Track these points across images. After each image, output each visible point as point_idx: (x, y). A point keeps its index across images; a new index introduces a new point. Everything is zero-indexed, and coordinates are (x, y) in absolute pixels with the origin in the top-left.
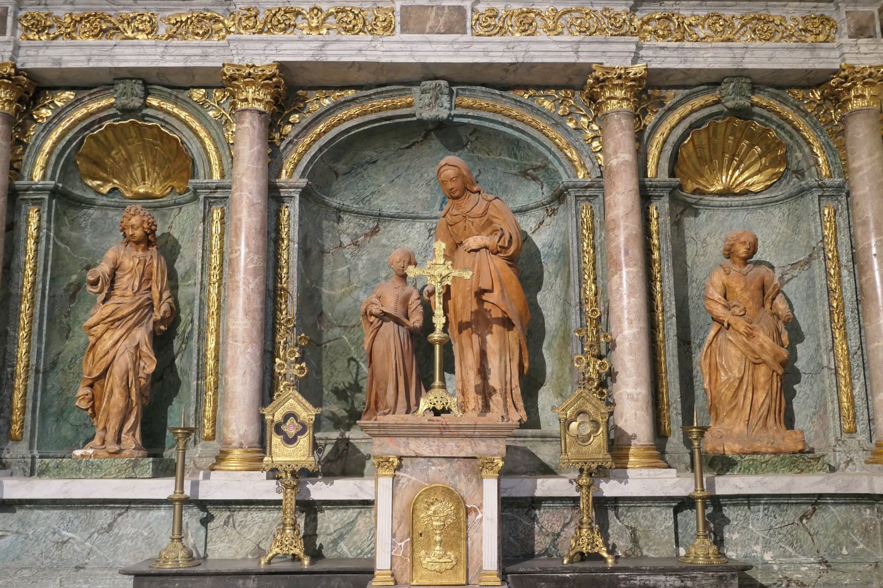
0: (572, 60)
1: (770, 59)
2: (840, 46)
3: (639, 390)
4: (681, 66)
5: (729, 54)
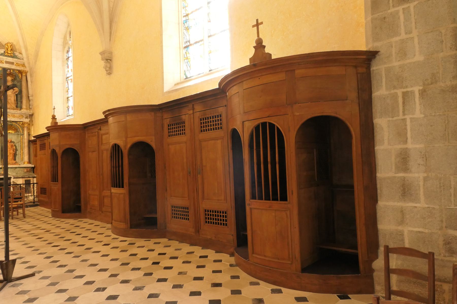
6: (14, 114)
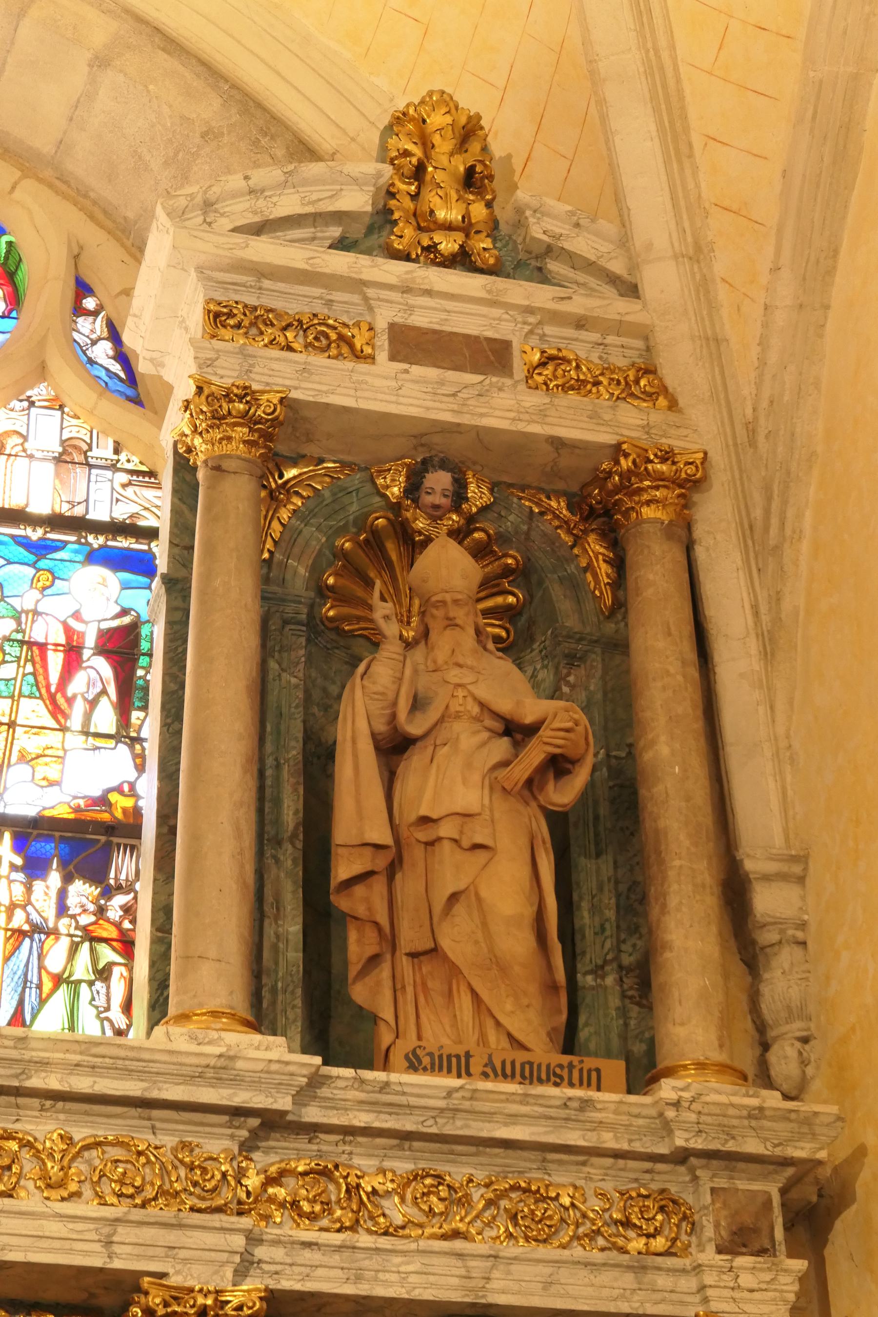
0: (97, 1262)
1: (547, 1285)
2: (698, 1268)
4: (349, 1289)
5: (456, 1267)
6: (536, 1177)
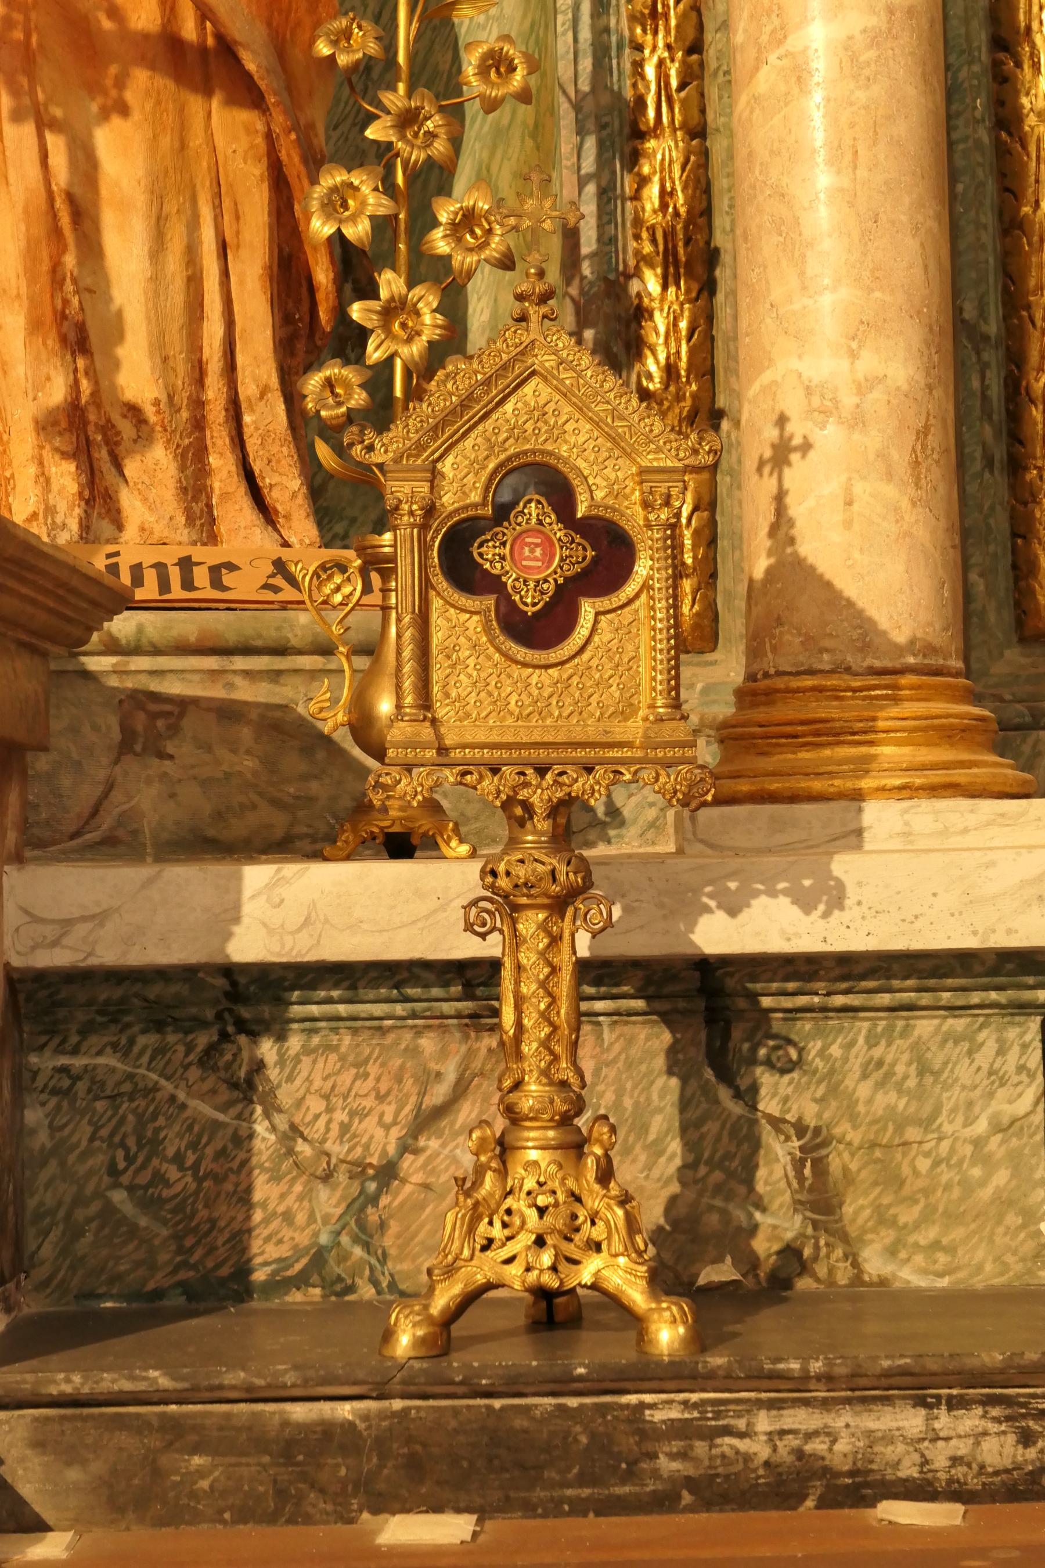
3: (868, 363)
